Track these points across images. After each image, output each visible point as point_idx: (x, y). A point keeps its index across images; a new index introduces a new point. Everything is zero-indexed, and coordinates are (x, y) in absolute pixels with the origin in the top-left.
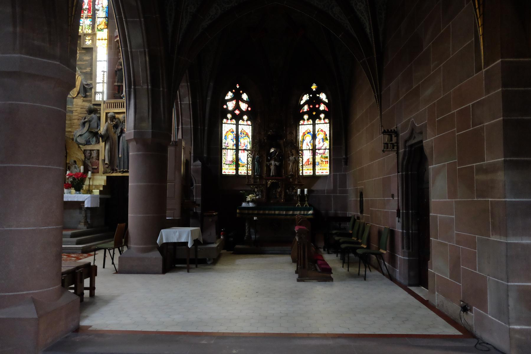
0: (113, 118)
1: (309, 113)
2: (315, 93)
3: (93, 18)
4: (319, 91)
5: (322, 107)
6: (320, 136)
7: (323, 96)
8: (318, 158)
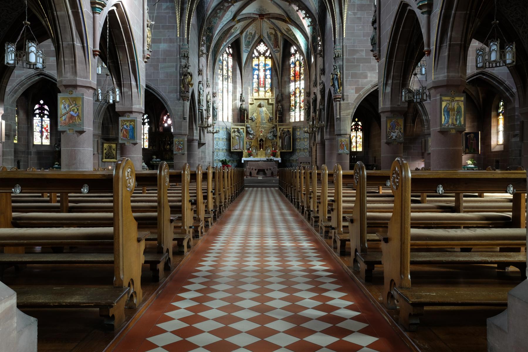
0: (283, 130)
1: (355, 129)
2: (357, 122)
3: (265, 87)
4: (358, 121)
5: (360, 127)
6: (358, 138)
7: (360, 123)
8: (358, 145)
